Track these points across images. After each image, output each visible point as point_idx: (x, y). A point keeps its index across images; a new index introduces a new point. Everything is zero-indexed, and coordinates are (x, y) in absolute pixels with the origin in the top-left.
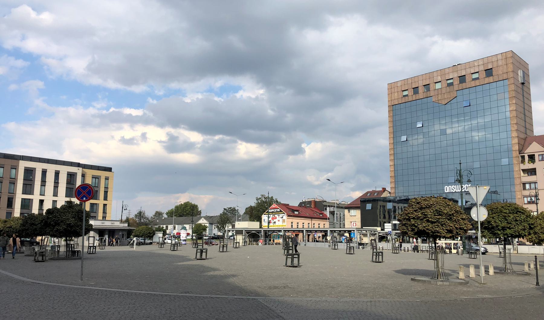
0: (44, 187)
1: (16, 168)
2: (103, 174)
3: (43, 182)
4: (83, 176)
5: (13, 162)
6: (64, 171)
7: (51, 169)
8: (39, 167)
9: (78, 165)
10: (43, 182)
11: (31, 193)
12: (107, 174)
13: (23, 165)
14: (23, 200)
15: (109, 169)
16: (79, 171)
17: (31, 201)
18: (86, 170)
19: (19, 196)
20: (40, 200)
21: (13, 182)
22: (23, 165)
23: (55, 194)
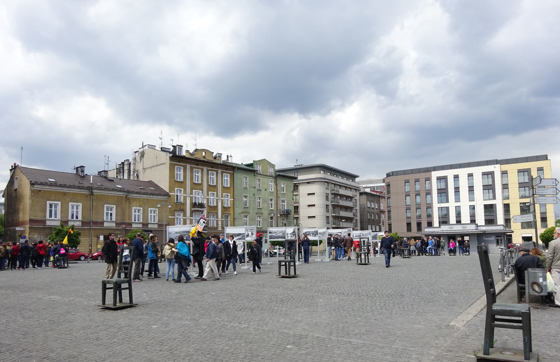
1: (429, 179)
2: (533, 166)
4: (504, 173)
5: (426, 175)
7: (463, 173)
8: (450, 174)
11: (447, 201)
12: (540, 164)
14: (440, 209)
15: (545, 158)
16: (497, 169)
17: (447, 208)
19: (436, 206)
20: (486, 206)
21: (429, 193)
22: (434, 175)
23: (472, 199)
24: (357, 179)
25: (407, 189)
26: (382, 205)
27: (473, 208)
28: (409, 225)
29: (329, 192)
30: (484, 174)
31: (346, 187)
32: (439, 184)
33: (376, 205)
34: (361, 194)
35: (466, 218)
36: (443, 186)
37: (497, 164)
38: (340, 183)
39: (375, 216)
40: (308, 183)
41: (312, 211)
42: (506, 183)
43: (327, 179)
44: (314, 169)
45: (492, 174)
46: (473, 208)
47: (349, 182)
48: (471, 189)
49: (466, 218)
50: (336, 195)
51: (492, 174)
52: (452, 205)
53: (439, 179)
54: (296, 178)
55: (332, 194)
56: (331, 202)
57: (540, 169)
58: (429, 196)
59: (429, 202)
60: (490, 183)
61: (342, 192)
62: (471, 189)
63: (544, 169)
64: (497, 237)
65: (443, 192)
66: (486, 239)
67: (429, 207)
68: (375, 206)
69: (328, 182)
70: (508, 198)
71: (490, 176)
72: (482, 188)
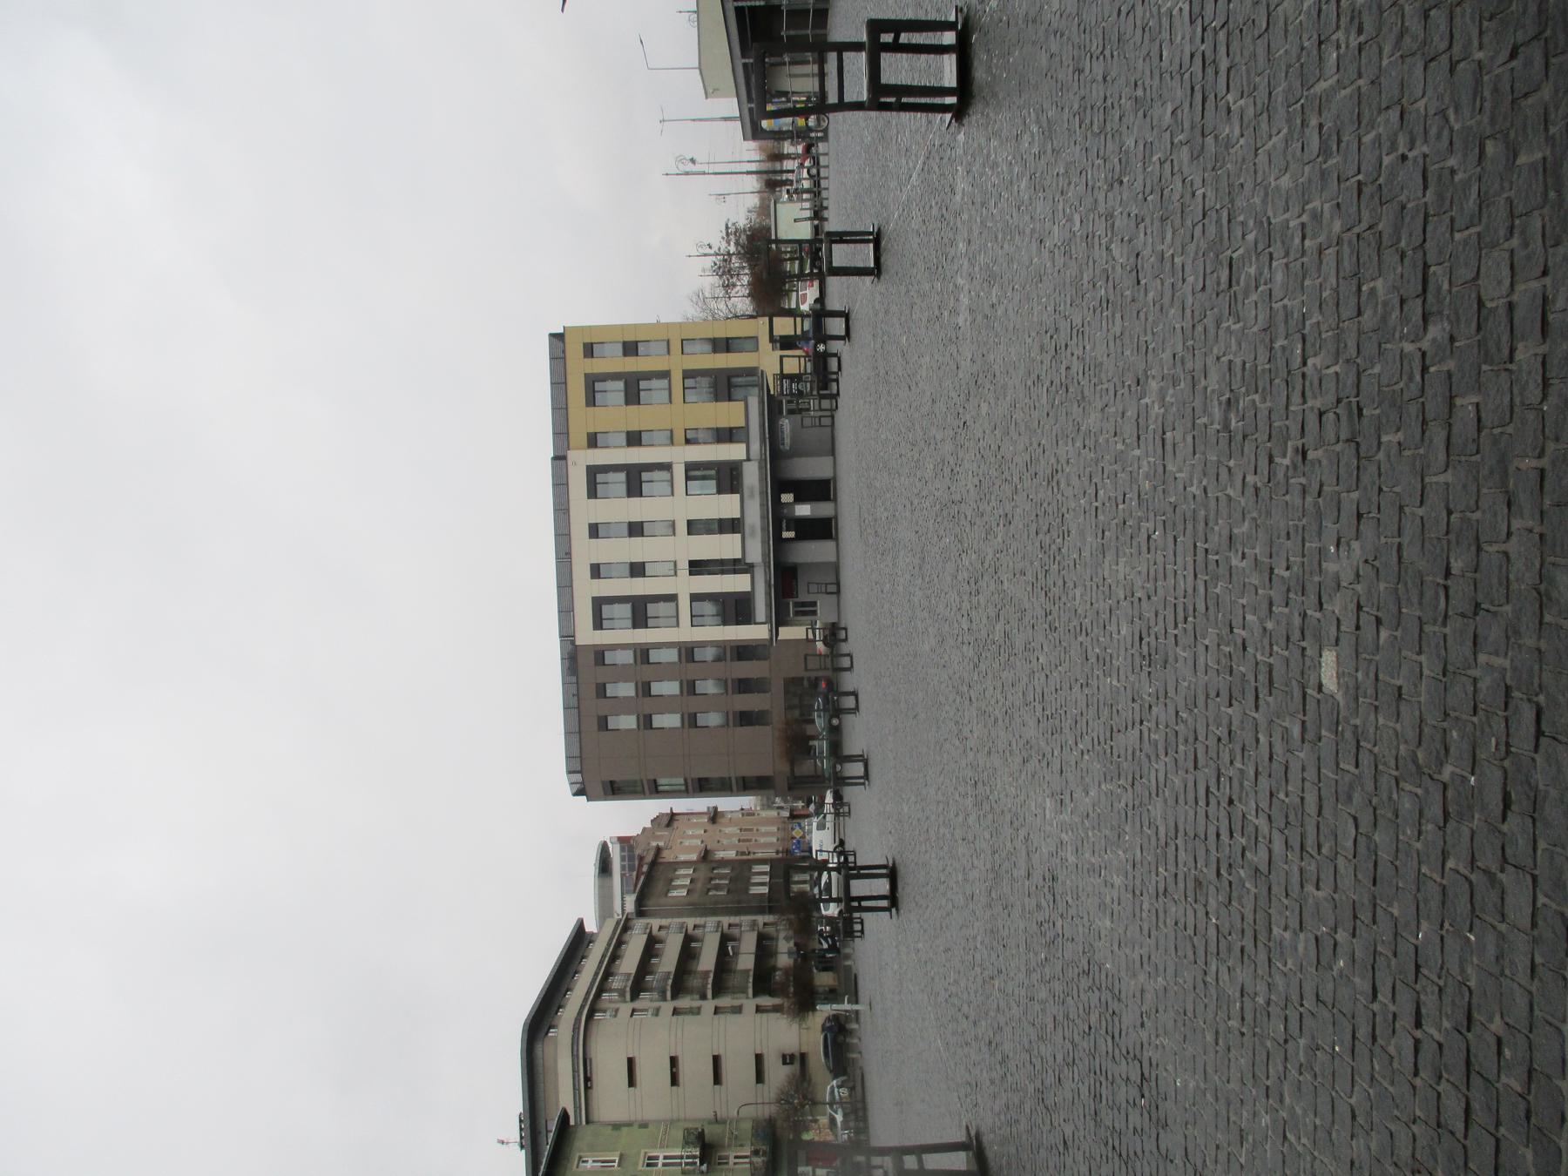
0: (649, 569)
1: (599, 654)
2: (578, 367)
3: (637, 570)
4: (593, 441)
5: (586, 661)
6: (584, 511)
7: (586, 551)
9: (559, 458)
10: (637, 570)
11: (672, 598)
12: (574, 350)
13: (587, 635)
15: (558, 338)
16: (581, 459)
17: (695, 598)
18: (578, 435)
19: (686, 633)
21: (643, 653)
24: (591, 927)
25: (628, 722)
26: (682, 858)
27: (694, 527)
28: (746, 719)
29: (626, 1008)
30: (592, 493)
31: (615, 956)
32: (616, 623)
33: (682, 872)
34: (640, 913)
35: (726, 546)
36: (625, 610)
37: (564, 458)
38: (596, 974)
39: (722, 877)
40: (587, 1088)
41: (696, 1070)
42: (623, 437)
43: (580, 1013)
44: (539, 1062)
45: (593, 472)
46: (694, 527)
47: (596, 953)
48: (636, 529)
49: (726, 546)
50: (638, 986)
51: (593, 472)
52: (687, 585)
53: (598, 624)
54: (565, 1116)
55: (635, 995)
56: (665, 999)
57: (589, 350)
58: (654, 656)
59: (671, 656)
60: (622, 476)
61: (629, 963)
62: (636, 529)
63: (588, 340)
64: (781, 412)
65: (640, 612)
66: (787, 441)
67: (688, 651)
68: (685, 876)
69: (593, 1009)
70: (673, 524)
71: (600, 478)
72: (635, 500)
